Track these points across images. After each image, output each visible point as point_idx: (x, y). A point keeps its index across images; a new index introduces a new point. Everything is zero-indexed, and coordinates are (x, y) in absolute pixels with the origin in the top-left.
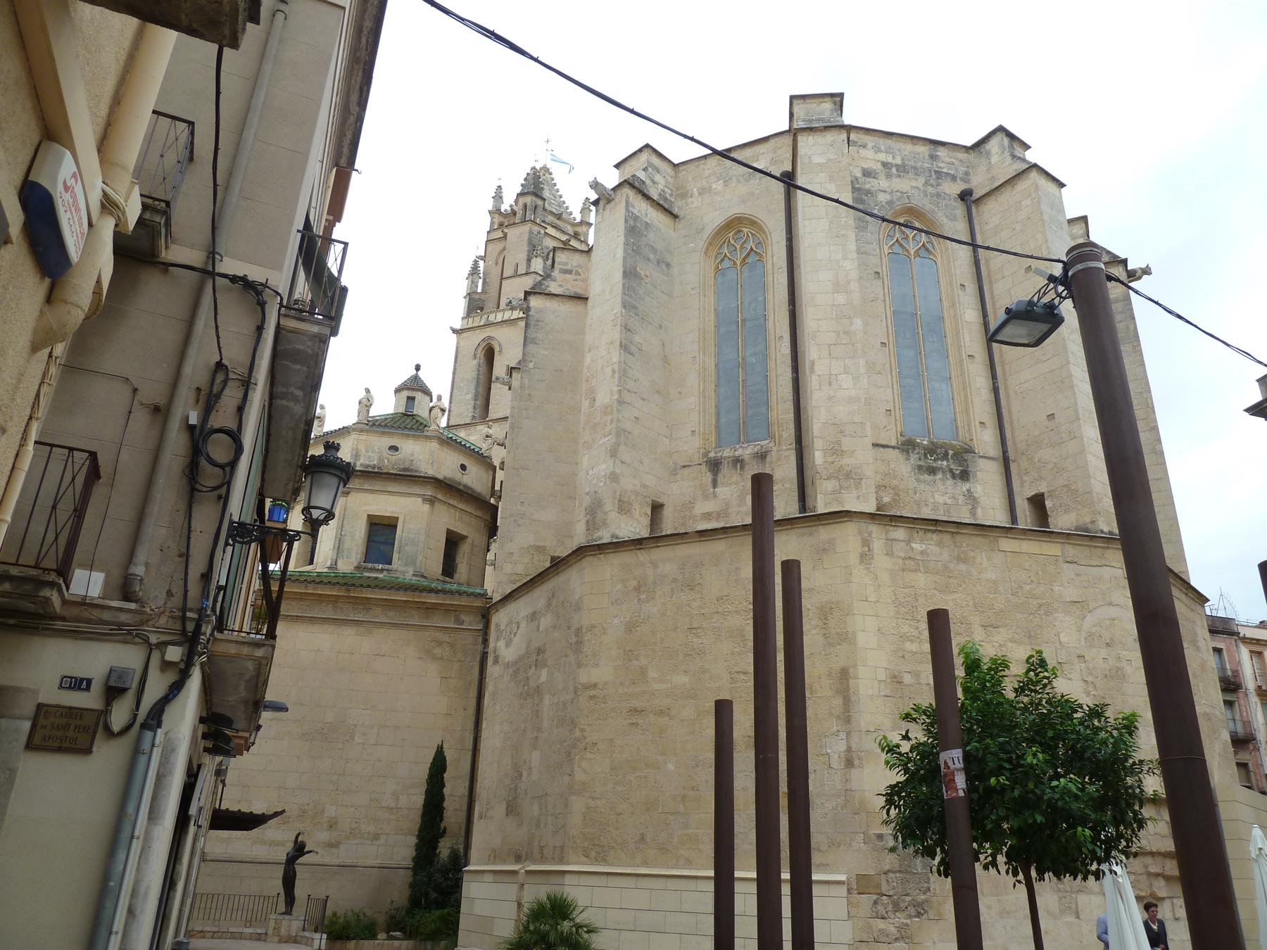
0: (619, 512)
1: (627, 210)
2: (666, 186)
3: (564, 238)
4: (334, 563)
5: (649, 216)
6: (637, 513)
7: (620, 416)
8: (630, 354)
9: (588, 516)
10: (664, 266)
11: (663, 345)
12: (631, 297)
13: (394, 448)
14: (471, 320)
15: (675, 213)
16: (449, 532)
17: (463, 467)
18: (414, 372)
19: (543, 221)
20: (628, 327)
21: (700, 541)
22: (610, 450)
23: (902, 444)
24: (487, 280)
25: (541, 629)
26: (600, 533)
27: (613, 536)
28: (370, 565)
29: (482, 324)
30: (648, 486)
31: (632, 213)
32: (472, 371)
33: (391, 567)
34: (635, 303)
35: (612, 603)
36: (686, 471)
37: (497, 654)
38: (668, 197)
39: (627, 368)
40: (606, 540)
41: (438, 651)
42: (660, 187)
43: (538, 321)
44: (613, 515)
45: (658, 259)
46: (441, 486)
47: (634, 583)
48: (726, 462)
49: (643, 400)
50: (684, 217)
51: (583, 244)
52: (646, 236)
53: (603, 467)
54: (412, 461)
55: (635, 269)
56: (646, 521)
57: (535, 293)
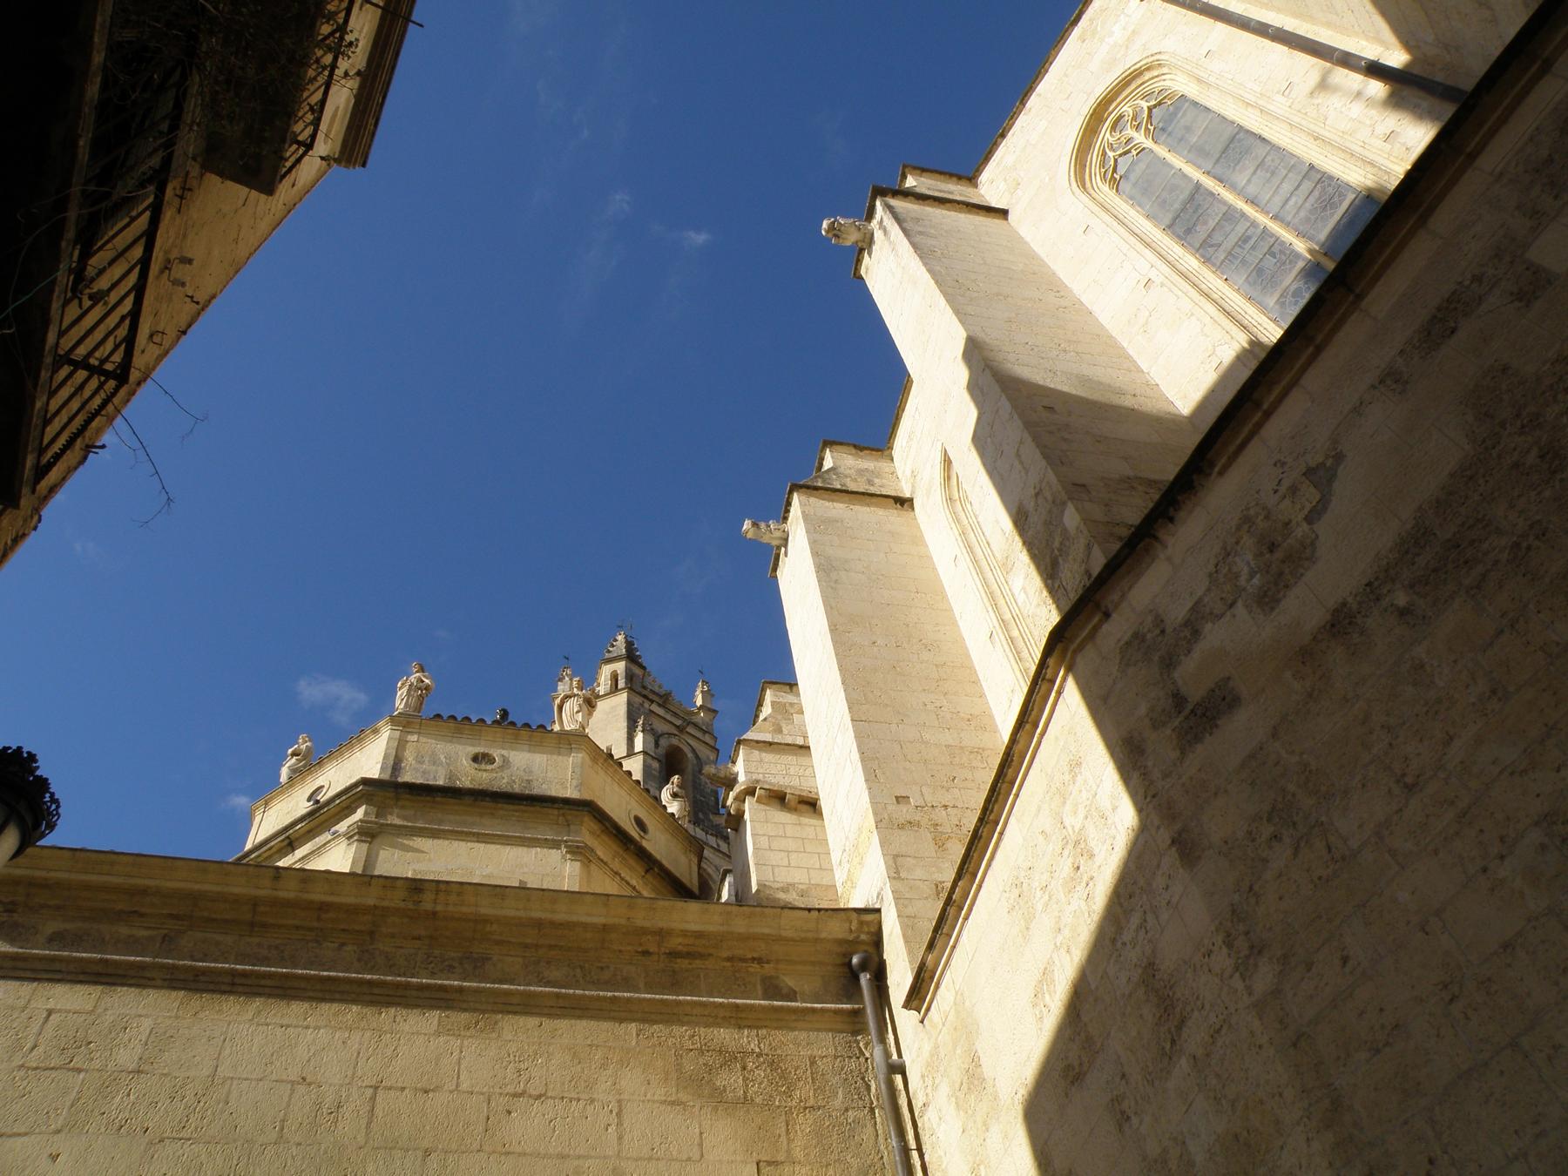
41: (730, 1080)
51: (707, 735)
54: (529, 781)
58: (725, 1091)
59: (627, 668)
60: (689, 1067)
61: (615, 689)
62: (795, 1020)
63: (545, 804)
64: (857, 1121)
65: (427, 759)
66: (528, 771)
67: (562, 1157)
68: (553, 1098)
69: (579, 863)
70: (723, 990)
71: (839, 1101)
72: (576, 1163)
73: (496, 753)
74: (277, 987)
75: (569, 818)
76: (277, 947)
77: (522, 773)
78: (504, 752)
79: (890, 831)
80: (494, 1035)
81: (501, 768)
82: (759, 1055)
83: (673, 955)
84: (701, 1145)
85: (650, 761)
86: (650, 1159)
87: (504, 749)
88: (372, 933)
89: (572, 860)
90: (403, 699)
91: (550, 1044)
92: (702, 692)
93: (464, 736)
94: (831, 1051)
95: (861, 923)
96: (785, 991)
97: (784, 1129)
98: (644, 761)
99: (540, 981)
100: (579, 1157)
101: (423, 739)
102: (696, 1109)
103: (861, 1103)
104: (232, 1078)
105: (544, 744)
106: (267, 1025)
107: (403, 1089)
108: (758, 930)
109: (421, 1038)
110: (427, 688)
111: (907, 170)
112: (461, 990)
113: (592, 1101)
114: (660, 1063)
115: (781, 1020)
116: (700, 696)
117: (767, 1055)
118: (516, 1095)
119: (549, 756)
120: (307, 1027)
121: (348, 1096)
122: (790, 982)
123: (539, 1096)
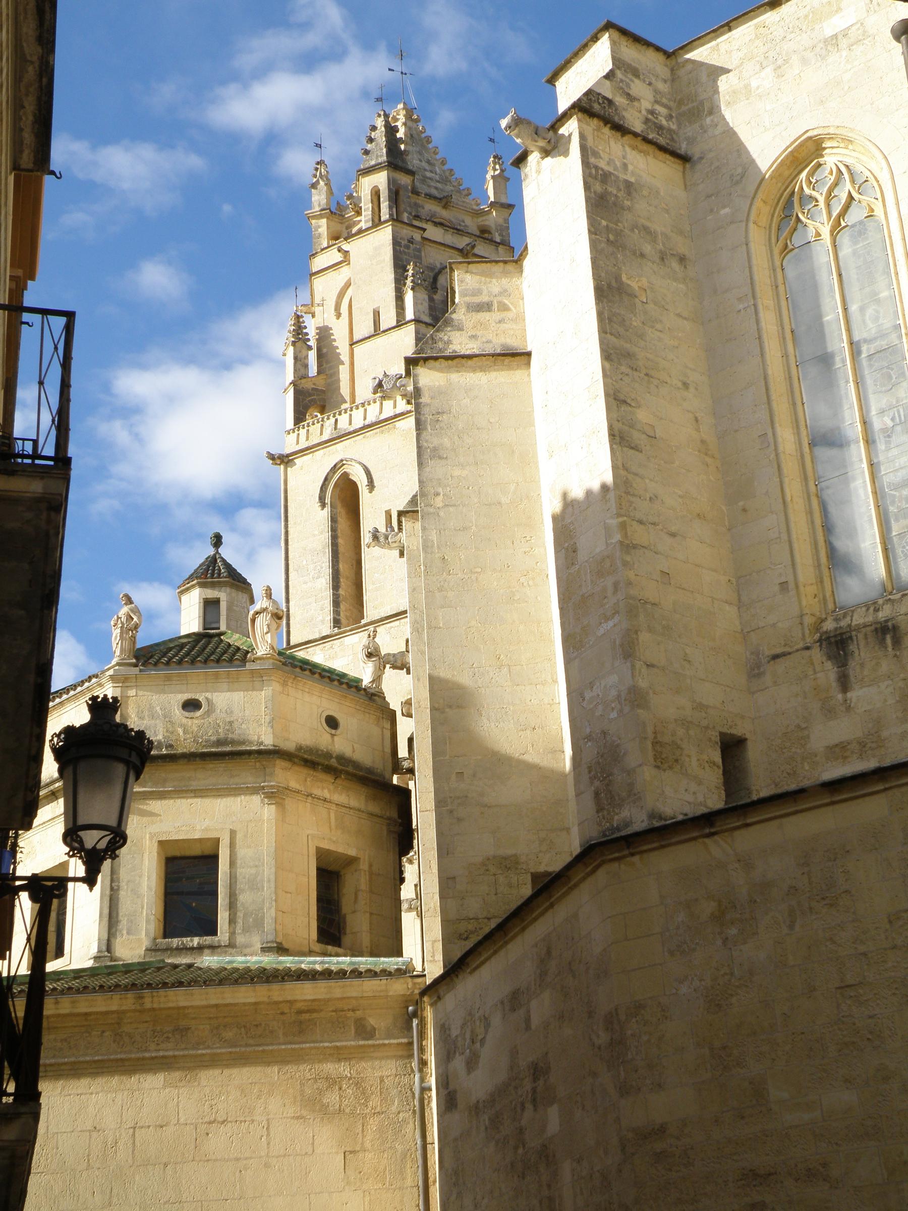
0: (657, 767)
2: (656, 102)
3: (462, 242)
4: (104, 948)
5: (630, 167)
6: (694, 763)
7: (631, 574)
8: (632, 448)
9: (597, 783)
10: (675, 265)
11: (697, 420)
12: (618, 336)
13: (191, 705)
14: (303, 432)
15: (682, 151)
16: (322, 855)
17: (332, 723)
18: (211, 551)
19: (417, 217)
20: (622, 397)
21: (833, 803)
22: (622, 645)
24: (325, 350)
25: (533, 1027)
26: (625, 813)
27: (652, 816)
28: (175, 942)
29: (326, 437)
30: (707, 707)
31: (596, 168)
32: (321, 533)
33: (216, 939)
34: (628, 346)
35: (672, 953)
36: (781, 666)
37: (451, 1087)
38: (664, 122)
39: (630, 477)
40: (640, 823)
41: (332, 1098)
42: (646, 104)
43: (438, 413)
44: (648, 773)
45: (661, 251)
46: (294, 763)
47: (708, 908)
48: (861, 636)
49: (673, 535)
50: (701, 158)
51: (501, 248)
52: (629, 209)
53: (614, 679)
54: (231, 723)
55: (618, 278)
56: (714, 777)
57: (426, 359)
58: (328, 1106)
59: (391, 182)
60: (308, 1091)
61: (377, 222)
62: (373, 1052)
63: (244, 757)
64: (404, 1120)
65: (147, 714)
66: (230, 712)
67: (237, 1159)
68: (231, 1122)
69: (273, 806)
70: (330, 1033)
71: (394, 1108)
72: (245, 1162)
73: (201, 698)
74: (71, 1070)
75: (264, 763)
76: (66, 1040)
77: (223, 715)
78: (208, 695)
79: (433, 918)
80: (196, 1084)
81: (209, 713)
82: (350, 1079)
83: (300, 1012)
84: (313, 1144)
85: (423, 328)
86: (285, 1156)
87: (207, 691)
88: (118, 1024)
89: (269, 804)
90: (118, 644)
91: (228, 1085)
92: (493, 177)
93: (174, 682)
94: (394, 1071)
95: (414, 984)
96: (369, 1028)
97: (361, 1129)
98: (417, 332)
99: (221, 1041)
100: (246, 1159)
101: (141, 693)
102: (311, 1120)
103: (408, 1107)
104: (57, 1133)
105: (240, 680)
106: (70, 1095)
107: (149, 1127)
108: (349, 995)
109: (156, 1090)
110: (136, 627)
111: (454, 266)
112: (175, 1056)
113: (253, 1121)
114: (291, 1091)
115: (364, 1052)
116: (491, 182)
117: (355, 1078)
118: (210, 1123)
119: (246, 693)
120: (92, 1094)
121: (120, 1135)
122: (372, 1021)
123: (223, 1122)
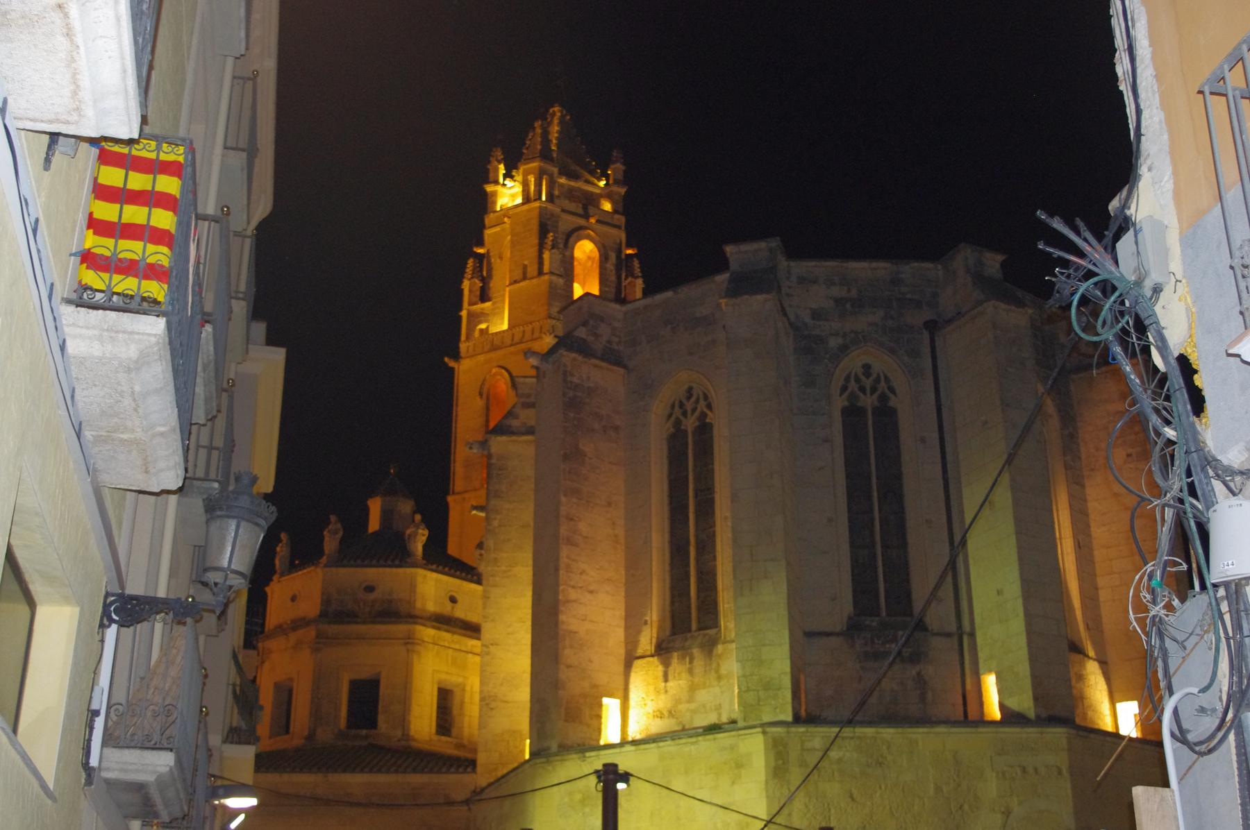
1: (565, 381)
23: (848, 629)
28: (353, 732)
31: (571, 382)
